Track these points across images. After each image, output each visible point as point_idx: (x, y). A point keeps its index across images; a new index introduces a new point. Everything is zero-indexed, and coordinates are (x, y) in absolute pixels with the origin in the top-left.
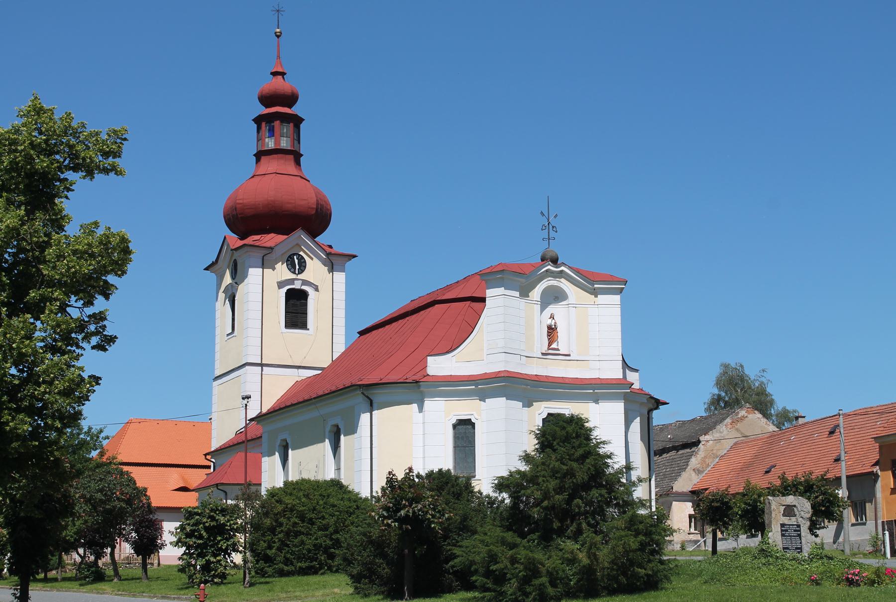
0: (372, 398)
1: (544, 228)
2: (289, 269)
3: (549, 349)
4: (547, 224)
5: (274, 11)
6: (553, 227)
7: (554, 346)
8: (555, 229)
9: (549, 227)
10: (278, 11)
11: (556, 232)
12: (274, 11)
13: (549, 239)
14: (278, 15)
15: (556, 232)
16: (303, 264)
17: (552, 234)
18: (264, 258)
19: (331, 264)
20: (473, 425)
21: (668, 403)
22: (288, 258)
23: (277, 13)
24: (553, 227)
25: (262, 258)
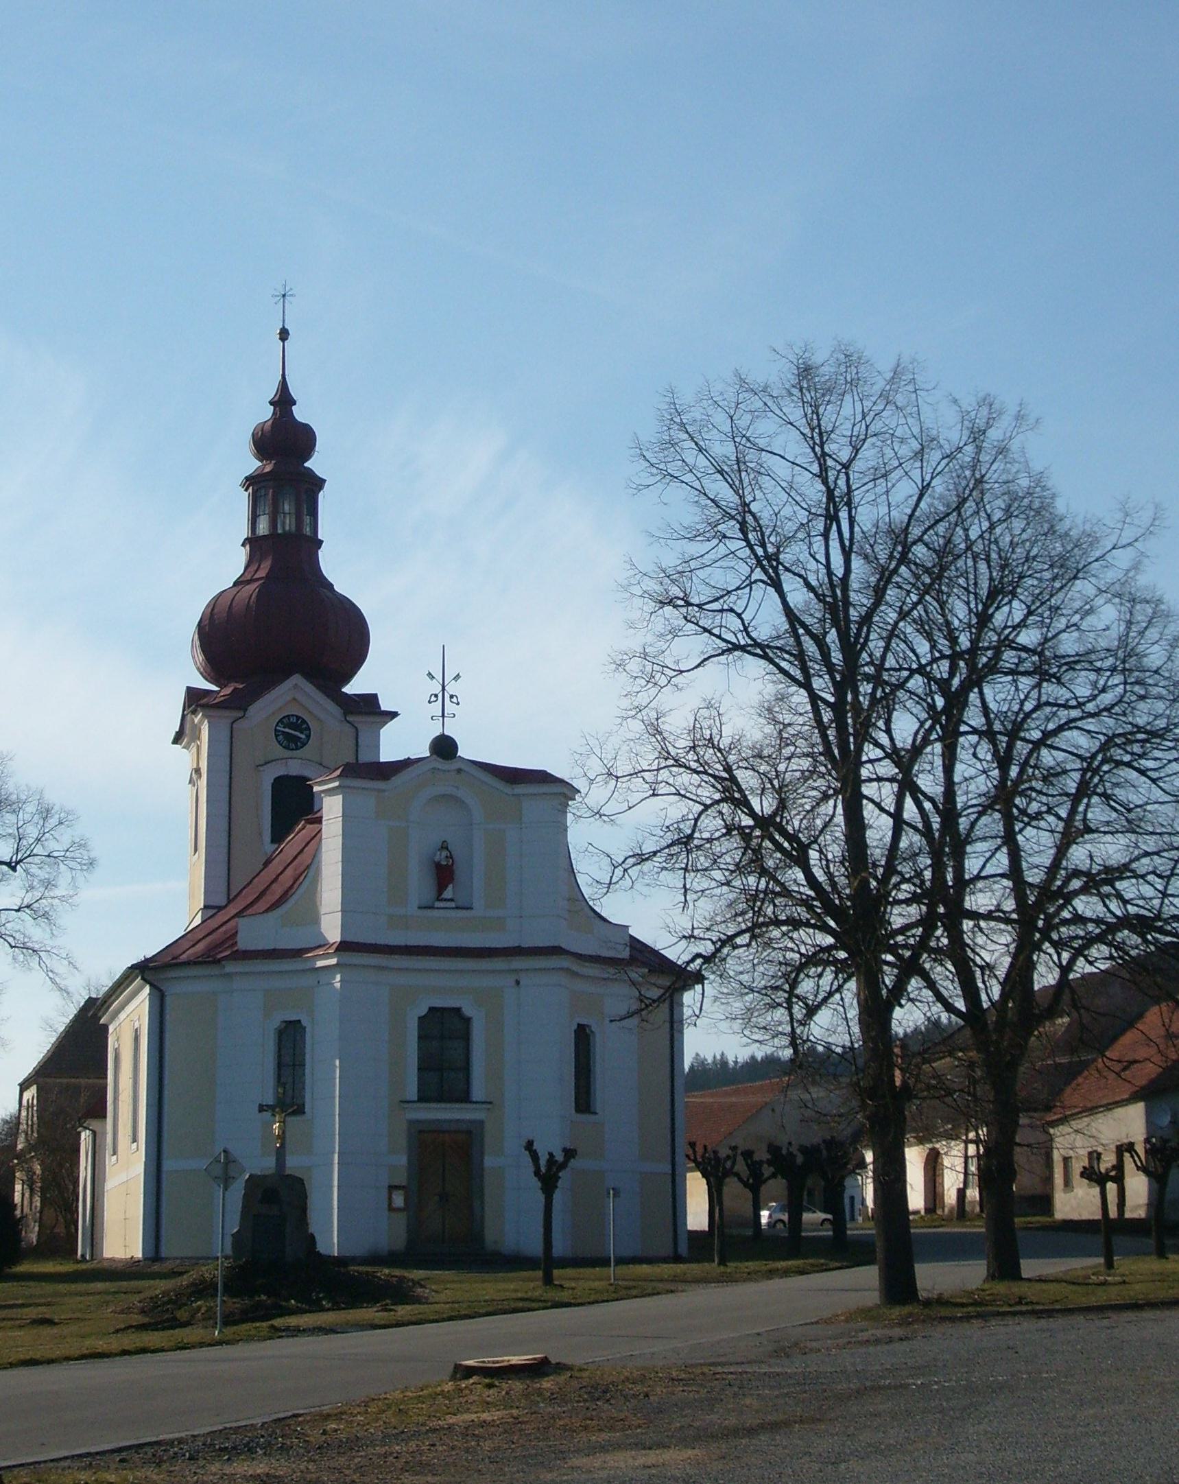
1: (433, 699)
2: (279, 742)
3: (439, 899)
6: (452, 697)
7: (448, 893)
8: (454, 700)
10: (284, 296)
11: (458, 704)
13: (443, 716)
14: (284, 302)
15: (458, 704)
24: (452, 697)
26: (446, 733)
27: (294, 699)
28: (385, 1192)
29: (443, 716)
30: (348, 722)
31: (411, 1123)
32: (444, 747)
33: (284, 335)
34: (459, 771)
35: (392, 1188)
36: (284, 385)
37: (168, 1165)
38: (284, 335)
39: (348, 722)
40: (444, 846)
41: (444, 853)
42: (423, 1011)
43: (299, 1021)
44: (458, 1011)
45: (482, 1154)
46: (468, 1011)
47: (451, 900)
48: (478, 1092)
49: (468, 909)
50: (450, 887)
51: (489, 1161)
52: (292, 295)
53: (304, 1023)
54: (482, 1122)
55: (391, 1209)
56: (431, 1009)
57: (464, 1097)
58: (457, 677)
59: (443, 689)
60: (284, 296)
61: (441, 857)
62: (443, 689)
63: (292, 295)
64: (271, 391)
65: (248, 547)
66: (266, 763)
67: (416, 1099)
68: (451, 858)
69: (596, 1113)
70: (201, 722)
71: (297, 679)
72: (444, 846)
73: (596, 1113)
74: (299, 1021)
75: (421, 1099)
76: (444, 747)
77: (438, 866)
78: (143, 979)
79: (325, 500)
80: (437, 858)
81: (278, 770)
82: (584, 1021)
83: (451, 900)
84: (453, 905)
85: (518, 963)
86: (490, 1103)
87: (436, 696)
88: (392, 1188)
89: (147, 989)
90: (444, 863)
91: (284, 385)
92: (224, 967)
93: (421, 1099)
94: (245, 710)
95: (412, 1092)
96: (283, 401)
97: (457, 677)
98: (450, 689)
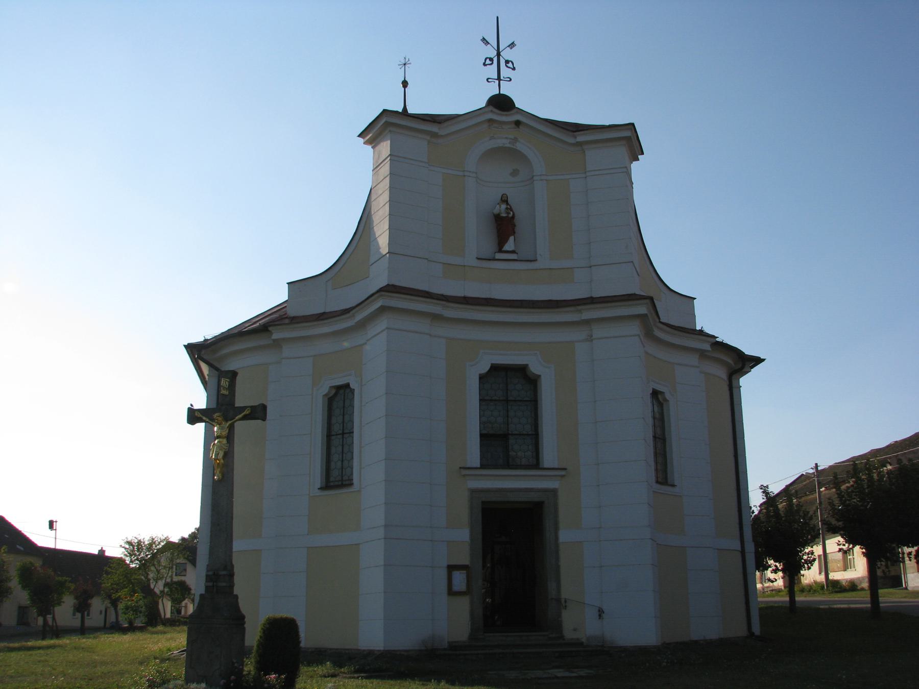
1: (488, 62)
3: (500, 250)
5: (401, 65)
6: (507, 62)
7: (510, 245)
8: (510, 65)
9: (497, 59)
10: (405, 64)
11: (514, 69)
12: (401, 65)
13: (499, 79)
15: (514, 69)
17: (505, 72)
20: (352, 391)
21: (763, 360)
23: (403, 67)
24: (507, 62)
26: (501, 93)
28: (443, 573)
29: (499, 79)
31: (473, 492)
32: (501, 103)
33: (405, 84)
34: (518, 123)
35: (451, 568)
38: (405, 84)
40: (504, 200)
41: (504, 206)
42: (485, 368)
44: (522, 370)
45: (556, 529)
46: (535, 368)
47: (513, 252)
49: (531, 261)
50: (512, 238)
51: (564, 536)
53: (352, 386)
54: (554, 492)
55: (451, 592)
56: (495, 368)
57: (535, 464)
58: (512, 45)
59: (499, 55)
60: (405, 64)
62: (499, 55)
67: (479, 466)
68: (511, 210)
69: (673, 486)
72: (504, 200)
73: (673, 486)
75: (483, 466)
76: (501, 103)
77: (498, 218)
80: (496, 211)
82: (659, 388)
83: (513, 252)
84: (514, 256)
86: (565, 469)
88: (451, 568)
90: (504, 215)
93: (483, 466)
95: (473, 456)
97: (512, 45)
98: (506, 54)
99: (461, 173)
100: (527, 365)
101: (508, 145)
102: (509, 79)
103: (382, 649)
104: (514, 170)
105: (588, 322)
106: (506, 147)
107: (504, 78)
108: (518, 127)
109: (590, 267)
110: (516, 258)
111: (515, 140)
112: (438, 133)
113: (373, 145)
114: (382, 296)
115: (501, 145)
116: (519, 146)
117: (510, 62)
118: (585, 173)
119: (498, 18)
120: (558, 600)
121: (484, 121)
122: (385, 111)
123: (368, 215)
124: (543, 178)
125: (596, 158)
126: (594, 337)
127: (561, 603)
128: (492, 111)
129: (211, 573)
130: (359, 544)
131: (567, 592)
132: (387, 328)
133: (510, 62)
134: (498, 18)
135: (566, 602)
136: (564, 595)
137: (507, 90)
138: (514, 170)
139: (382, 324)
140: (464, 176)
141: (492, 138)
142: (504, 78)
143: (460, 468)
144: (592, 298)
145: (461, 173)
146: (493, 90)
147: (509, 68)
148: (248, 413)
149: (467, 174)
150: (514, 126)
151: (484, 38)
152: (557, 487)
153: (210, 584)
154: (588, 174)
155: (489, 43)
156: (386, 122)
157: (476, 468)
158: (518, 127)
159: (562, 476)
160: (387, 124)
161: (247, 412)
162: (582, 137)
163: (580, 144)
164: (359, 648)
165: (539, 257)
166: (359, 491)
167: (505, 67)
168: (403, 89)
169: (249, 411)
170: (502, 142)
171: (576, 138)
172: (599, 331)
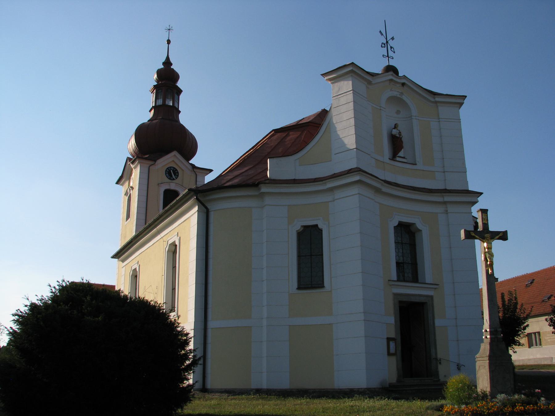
0: (209, 207)
1: (383, 46)
2: (166, 176)
4: (385, 42)
6: (391, 47)
7: (401, 154)
8: (392, 49)
10: (169, 30)
11: (394, 52)
16: (177, 174)
18: (151, 168)
19: (195, 175)
20: (321, 231)
22: (166, 169)
24: (391, 47)
25: (148, 167)
26: (390, 64)
27: (173, 161)
28: (385, 342)
30: (194, 172)
31: (395, 295)
33: (169, 42)
34: (403, 84)
35: (389, 339)
36: (168, 58)
37: (211, 324)
38: (169, 42)
39: (194, 172)
42: (396, 224)
43: (317, 225)
46: (419, 226)
48: (429, 278)
51: (438, 322)
52: (172, 30)
53: (320, 226)
54: (432, 297)
55: (389, 354)
58: (393, 38)
59: (387, 42)
61: (395, 132)
62: (387, 42)
63: (172, 30)
64: (164, 60)
65: (153, 111)
66: (162, 183)
70: (135, 168)
71: (175, 153)
72: (396, 127)
74: (317, 225)
78: (197, 199)
79: (182, 97)
81: (167, 187)
83: (404, 158)
85: (448, 198)
86: (438, 285)
87: (384, 44)
88: (389, 339)
89: (196, 208)
91: (168, 58)
92: (260, 189)
94: (155, 161)
95: (394, 275)
96: (167, 63)
98: (391, 43)
99: (379, 108)
100: (414, 224)
101: (398, 96)
102: (384, 56)
103: (365, 387)
104: (397, 110)
105: (445, 203)
106: (397, 97)
107: (386, 58)
108: (403, 87)
109: (444, 172)
110: (406, 162)
111: (402, 94)
112: (372, 82)
113: (332, 82)
114: (359, 174)
115: (395, 95)
116: (404, 98)
117: (393, 48)
118: (439, 119)
119: (385, 21)
120: (436, 359)
121: (387, 80)
122: (353, 63)
123: (329, 123)
124: (417, 118)
125: (444, 111)
126: (449, 211)
127: (438, 361)
128: (392, 75)
129: (492, 330)
130: (331, 324)
131: (440, 354)
132: (359, 194)
133: (393, 48)
134: (385, 21)
135: (440, 360)
136: (439, 356)
137: (392, 63)
138: (397, 110)
139: (355, 190)
140: (381, 109)
141: (391, 90)
142: (386, 58)
143: (389, 280)
144: (446, 189)
145: (379, 108)
146: (385, 63)
147: (392, 51)
148: (501, 235)
149: (382, 108)
150: (400, 85)
151: (380, 31)
152: (433, 294)
153: (493, 336)
154: (441, 120)
155: (383, 35)
156: (352, 70)
157: (395, 281)
158: (403, 87)
159: (435, 288)
160: (352, 71)
161: (501, 235)
162: (438, 99)
163: (436, 102)
164: (335, 388)
165: (417, 163)
166: (330, 291)
167: (391, 51)
168: (168, 45)
169: (502, 234)
170: (395, 94)
171: (435, 98)
172: (451, 209)
